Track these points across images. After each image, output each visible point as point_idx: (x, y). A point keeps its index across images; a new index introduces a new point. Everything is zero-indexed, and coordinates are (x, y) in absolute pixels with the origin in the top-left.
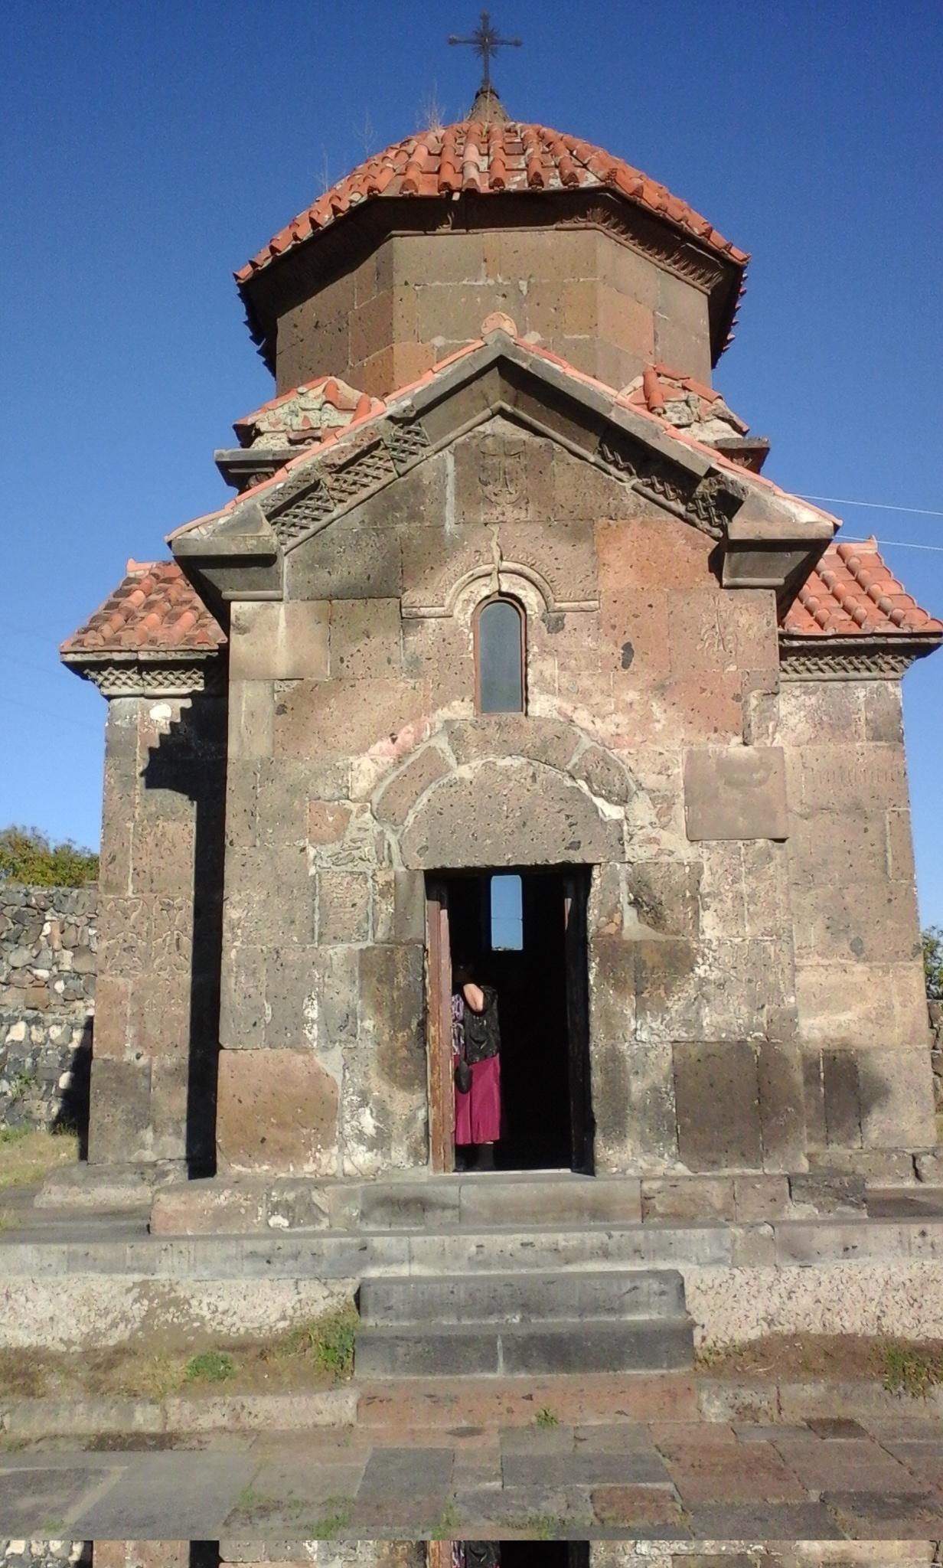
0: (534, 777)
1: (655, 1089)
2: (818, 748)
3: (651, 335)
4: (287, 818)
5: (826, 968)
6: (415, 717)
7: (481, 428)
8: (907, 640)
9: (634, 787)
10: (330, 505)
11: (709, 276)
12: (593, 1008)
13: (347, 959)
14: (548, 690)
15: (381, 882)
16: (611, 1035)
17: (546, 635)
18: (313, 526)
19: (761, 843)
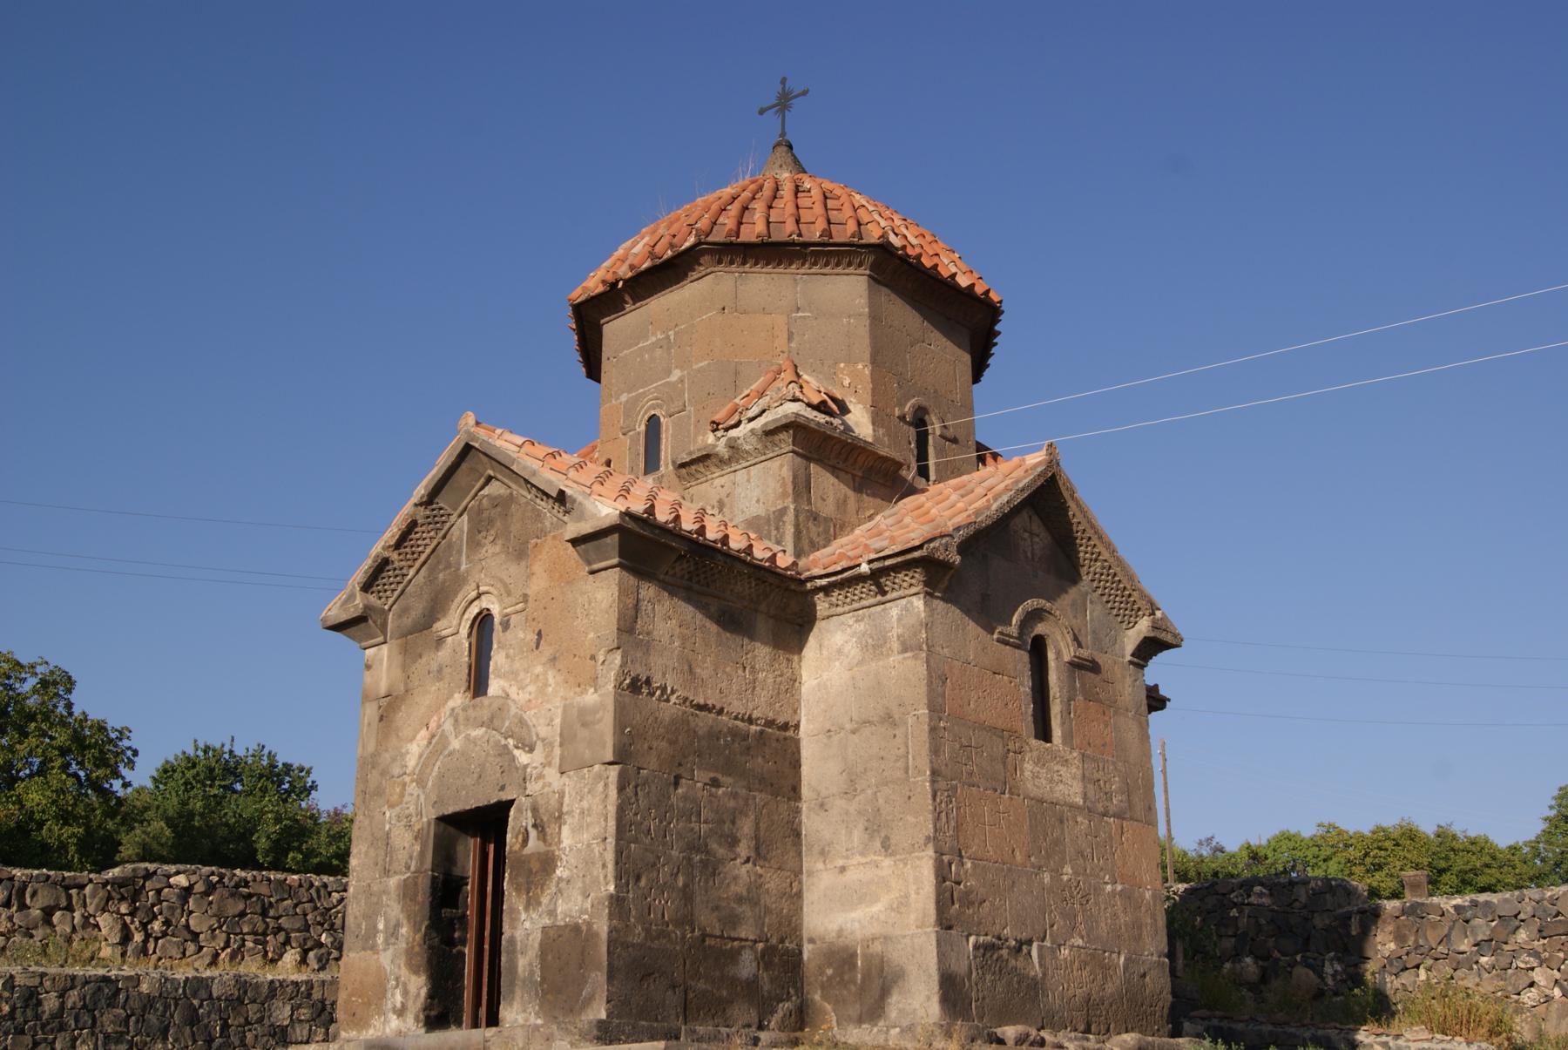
1: (530, 964)
2: (864, 668)
3: (786, 336)
7: (482, 492)
8: (899, 559)
9: (535, 738)
10: (404, 571)
14: (499, 676)
16: (514, 928)
17: (501, 634)
18: (401, 587)
19: (597, 767)
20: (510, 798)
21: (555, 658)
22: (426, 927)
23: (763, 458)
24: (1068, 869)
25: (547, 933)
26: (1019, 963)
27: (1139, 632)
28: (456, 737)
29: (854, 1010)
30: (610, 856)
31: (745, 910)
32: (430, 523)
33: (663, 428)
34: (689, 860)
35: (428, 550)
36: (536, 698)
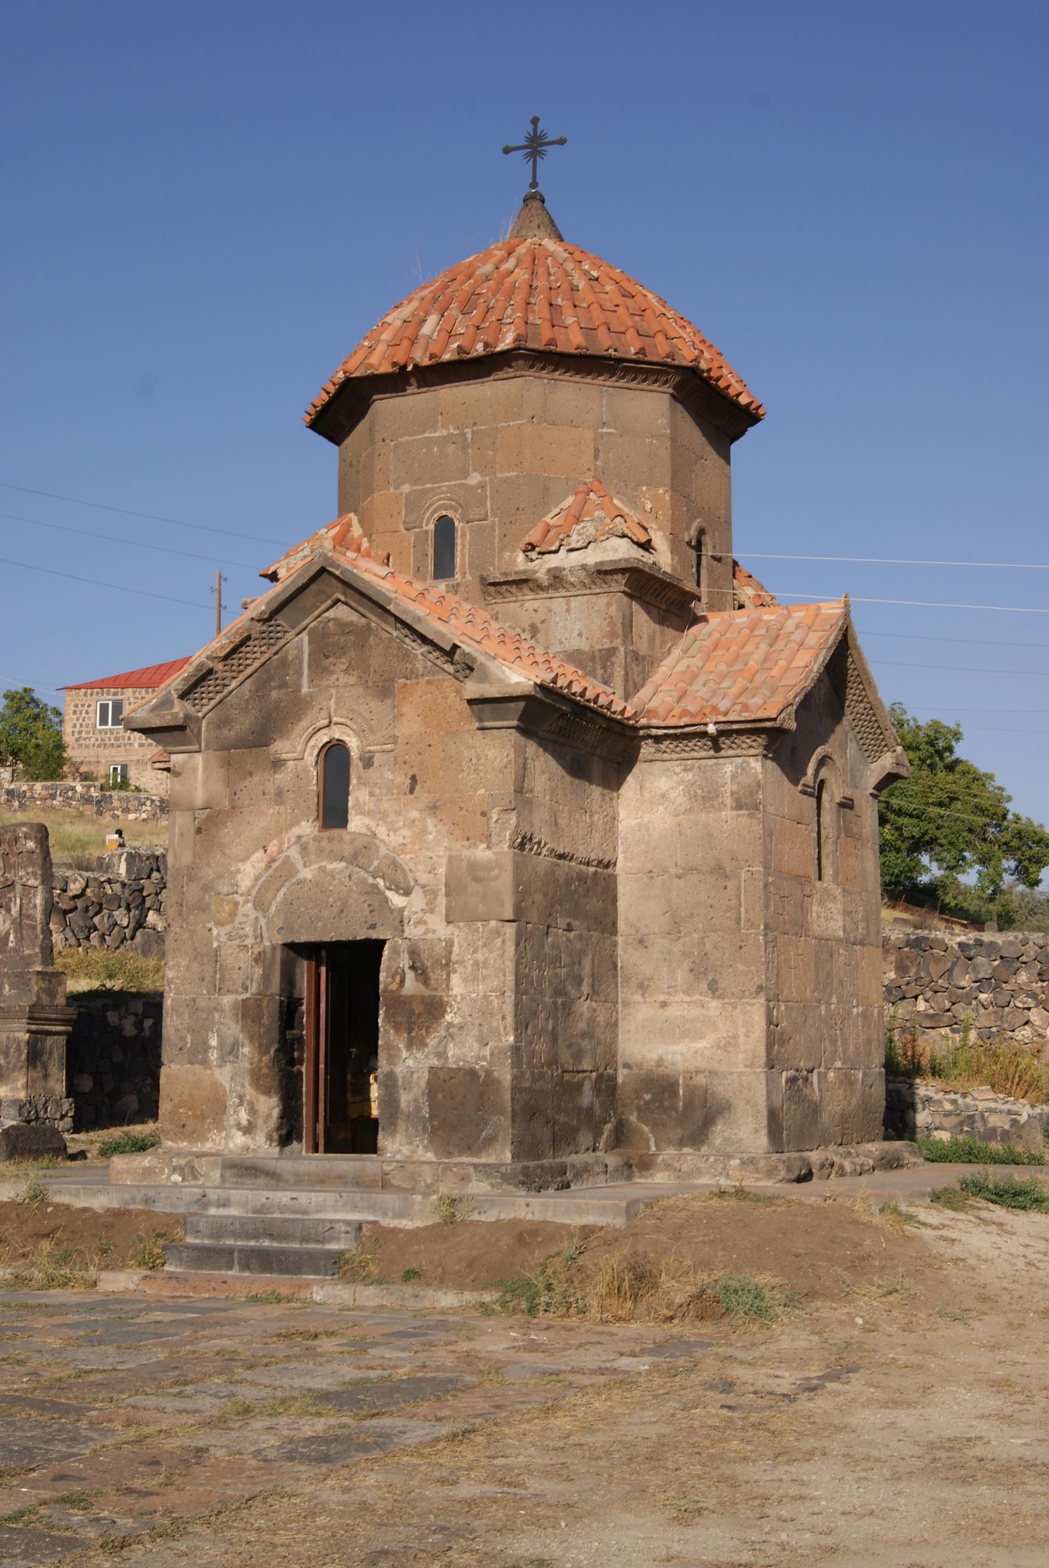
0: (350, 876)
1: (416, 1100)
2: (692, 817)
3: (592, 452)
4: (201, 907)
5: (689, 1003)
6: (279, 834)
7: (326, 614)
8: (749, 726)
10: (226, 682)
11: (663, 379)
12: (380, 1043)
13: (235, 1005)
14: (361, 812)
15: (256, 952)
17: (362, 770)
18: (219, 697)
20: (382, 937)
21: (435, 807)
22: (276, 1051)
23: (588, 591)
24: (834, 1000)
25: (435, 1074)
26: (806, 1091)
27: (883, 768)
28: (305, 866)
29: (676, 1133)
30: (509, 1009)
31: (585, 1044)
32: (263, 638)
33: (459, 534)
34: (555, 1003)
35: (256, 664)
36: (413, 843)
